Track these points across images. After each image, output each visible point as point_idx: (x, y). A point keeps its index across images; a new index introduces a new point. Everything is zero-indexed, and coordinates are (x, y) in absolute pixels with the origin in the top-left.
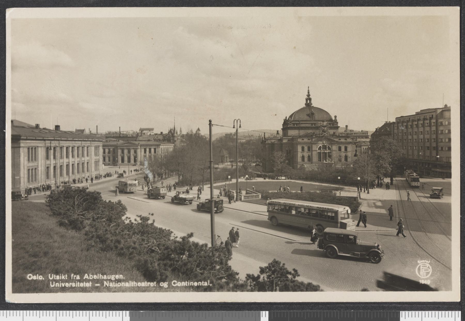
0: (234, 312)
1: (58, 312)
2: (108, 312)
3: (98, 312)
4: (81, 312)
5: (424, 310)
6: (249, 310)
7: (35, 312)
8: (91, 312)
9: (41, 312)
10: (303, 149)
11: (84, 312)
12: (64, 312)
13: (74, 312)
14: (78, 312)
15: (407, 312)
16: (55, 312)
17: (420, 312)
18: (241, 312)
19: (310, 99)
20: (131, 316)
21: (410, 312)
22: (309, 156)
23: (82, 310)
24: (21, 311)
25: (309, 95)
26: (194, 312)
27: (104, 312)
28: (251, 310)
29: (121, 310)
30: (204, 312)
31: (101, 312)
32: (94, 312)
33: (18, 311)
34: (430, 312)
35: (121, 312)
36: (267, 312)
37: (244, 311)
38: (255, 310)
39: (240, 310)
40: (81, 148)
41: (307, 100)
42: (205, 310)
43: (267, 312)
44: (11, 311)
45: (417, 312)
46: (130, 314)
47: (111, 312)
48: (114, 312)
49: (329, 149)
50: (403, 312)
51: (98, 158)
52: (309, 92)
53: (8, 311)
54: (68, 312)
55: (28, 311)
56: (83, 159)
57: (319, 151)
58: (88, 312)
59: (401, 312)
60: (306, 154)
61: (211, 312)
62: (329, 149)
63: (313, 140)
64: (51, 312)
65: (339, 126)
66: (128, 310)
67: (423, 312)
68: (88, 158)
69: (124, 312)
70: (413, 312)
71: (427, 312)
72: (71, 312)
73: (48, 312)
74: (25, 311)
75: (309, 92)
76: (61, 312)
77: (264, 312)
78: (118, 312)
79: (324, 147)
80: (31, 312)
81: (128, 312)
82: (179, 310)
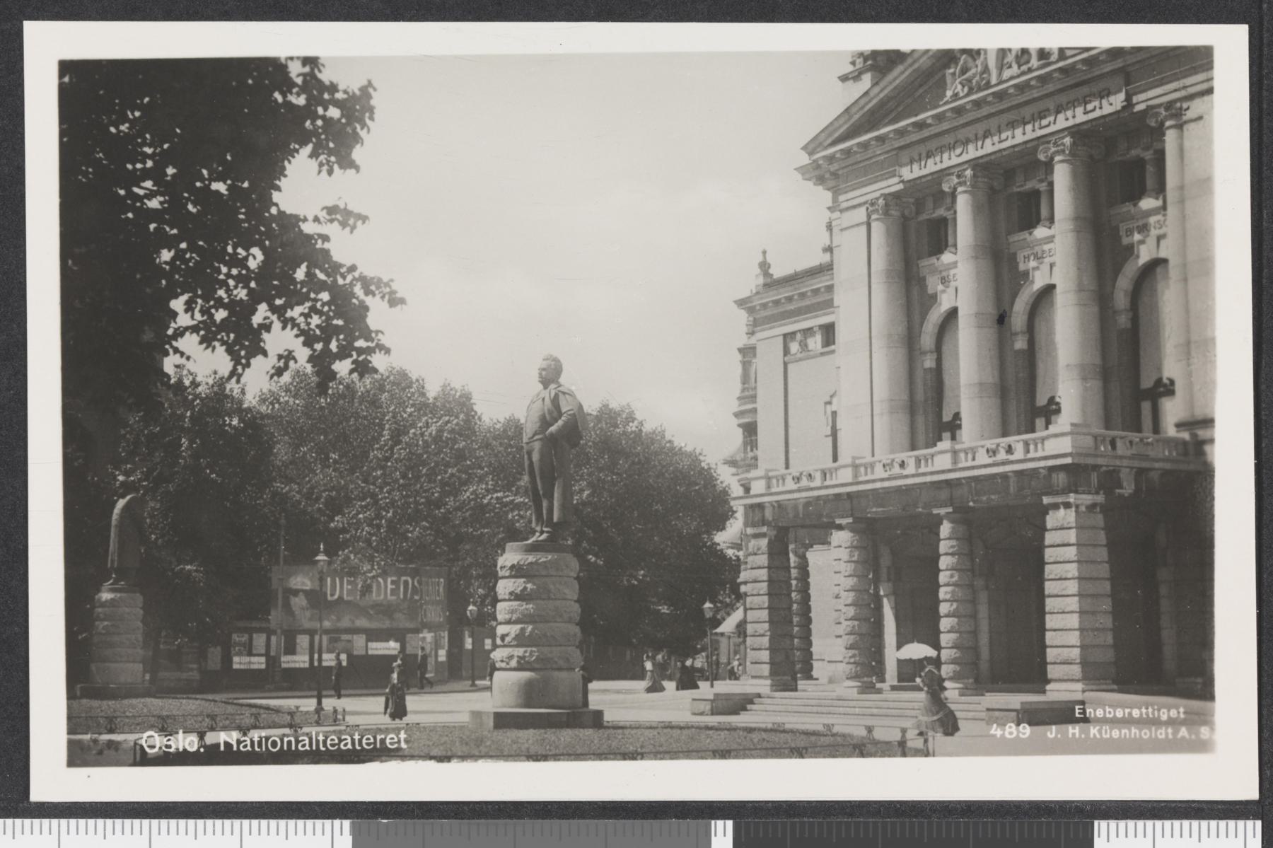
0: (638, 822)
1: (155, 822)
2: (291, 822)
3: (264, 822)
4: (218, 822)
6: (677, 817)
7: (91, 822)
8: (246, 822)
9: (109, 822)
11: (228, 822)
12: (173, 822)
13: (200, 822)
14: (209, 822)
16: (146, 822)
18: (656, 823)
20: (355, 833)
23: (223, 817)
24: (55, 822)
27: (282, 822)
28: (683, 818)
29: (328, 818)
30: (556, 823)
31: (273, 822)
32: (255, 822)
33: (46, 822)
35: (328, 822)
36: (730, 823)
37: (665, 823)
38: (696, 817)
39: (656, 818)
43: (730, 823)
44: (27, 822)
47: (300, 822)
48: (310, 822)
53: (18, 821)
54: (182, 822)
55: (73, 822)
58: (237, 822)
64: (137, 822)
66: (346, 818)
69: (337, 822)
72: (191, 822)
73: (128, 822)
74: (64, 822)
76: (164, 822)
77: (720, 823)
78: (319, 822)
80: (82, 822)
81: (347, 823)
82: (487, 818)
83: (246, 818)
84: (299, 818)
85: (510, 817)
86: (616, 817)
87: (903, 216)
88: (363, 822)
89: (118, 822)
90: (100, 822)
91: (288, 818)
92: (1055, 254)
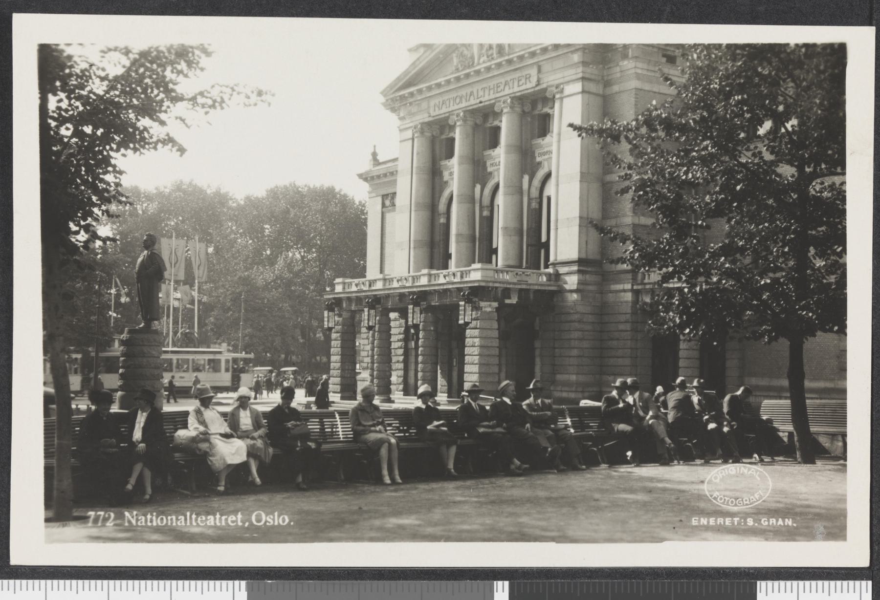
1: (112, 582)
2: (205, 582)
3: (187, 582)
4: (155, 582)
5: (802, 580)
8: (174, 582)
9: (80, 582)
11: (162, 582)
12: (124, 582)
13: (143, 582)
14: (149, 582)
15: (770, 583)
16: (105, 582)
17: (795, 583)
20: (249, 590)
21: (776, 583)
23: (158, 579)
26: (368, 583)
27: (199, 582)
30: (387, 583)
31: (193, 582)
32: (180, 582)
34: (814, 583)
35: (230, 583)
42: (390, 579)
45: (789, 583)
46: (247, 584)
47: (212, 582)
48: (218, 582)
50: (763, 583)
54: (130, 582)
58: (168, 582)
59: (758, 582)
61: (400, 582)
64: (99, 582)
66: (243, 579)
67: (801, 583)
69: (237, 582)
70: (782, 583)
71: (807, 583)
72: (137, 582)
76: (118, 582)
78: (224, 582)
83: (174, 579)
84: (210, 579)
85: (356, 579)
86: (429, 579)
87: (433, 136)
88: (255, 583)
89: (87, 582)
90: (74, 582)
91: (203, 579)
92: (501, 159)
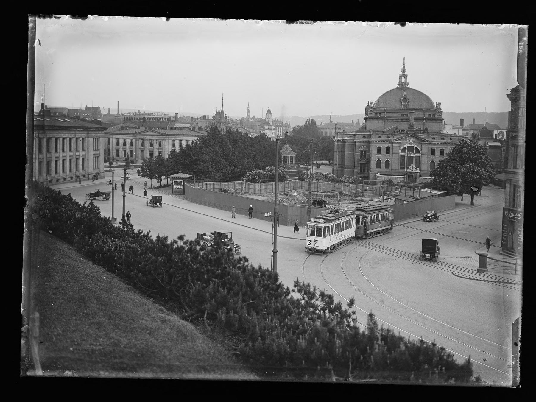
10: (379, 150)
19: (405, 77)
22: (387, 161)
25: (404, 71)
40: (74, 140)
41: (401, 77)
49: (417, 151)
51: (98, 152)
52: (404, 66)
56: (77, 154)
57: (403, 154)
60: (383, 157)
62: (417, 151)
63: (395, 137)
65: (443, 117)
68: (84, 153)
75: (404, 66)
79: (410, 149)
